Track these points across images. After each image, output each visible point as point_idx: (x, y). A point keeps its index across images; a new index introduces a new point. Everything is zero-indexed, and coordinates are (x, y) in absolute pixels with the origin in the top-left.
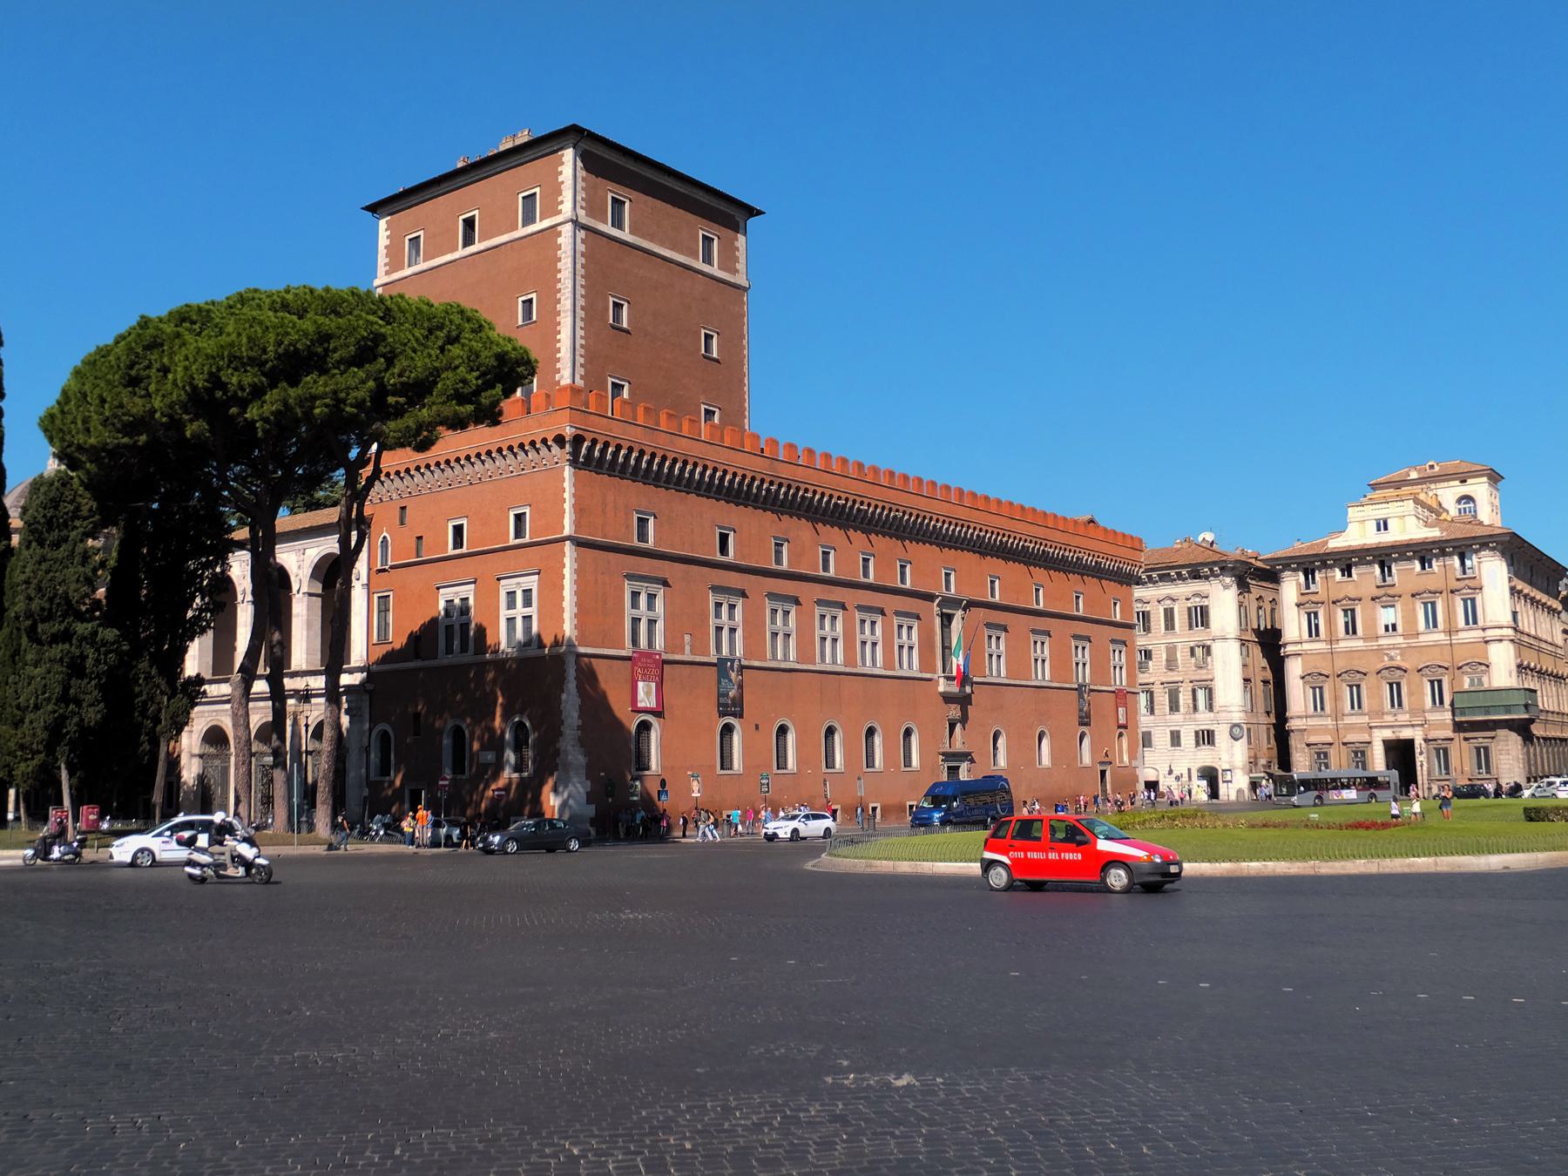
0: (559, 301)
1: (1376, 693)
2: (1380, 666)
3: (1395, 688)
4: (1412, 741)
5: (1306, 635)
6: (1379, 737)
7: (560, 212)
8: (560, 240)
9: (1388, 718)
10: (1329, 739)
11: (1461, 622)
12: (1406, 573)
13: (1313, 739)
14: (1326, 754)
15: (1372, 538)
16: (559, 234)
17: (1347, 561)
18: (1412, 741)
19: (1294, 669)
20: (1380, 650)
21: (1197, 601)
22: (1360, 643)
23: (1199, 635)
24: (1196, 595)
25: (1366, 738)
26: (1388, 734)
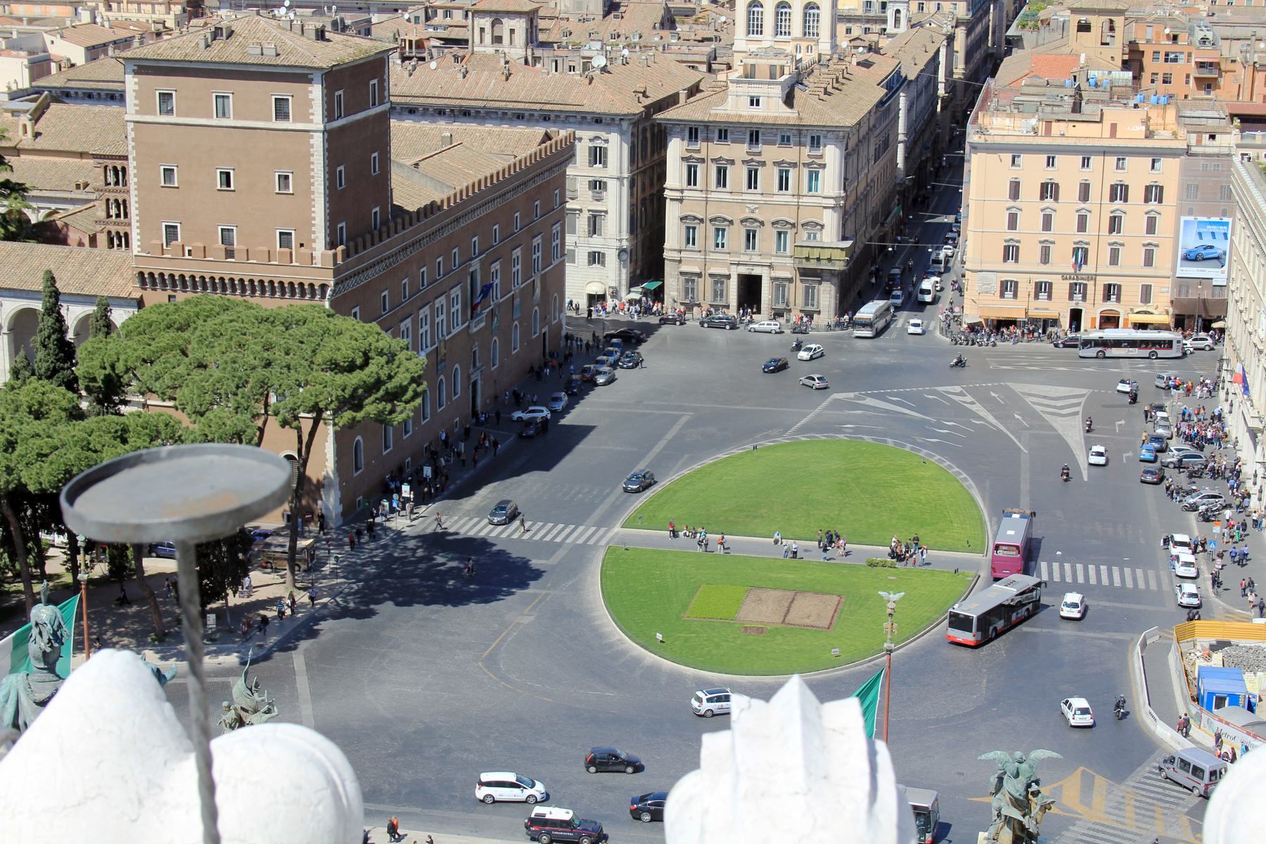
0: (313, 184)
1: (735, 236)
2: (743, 216)
3: (750, 237)
4: (760, 278)
5: (685, 185)
6: (735, 272)
7: (311, 121)
8: (312, 141)
9: (744, 259)
10: (698, 271)
11: (805, 190)
12: (771, 152)
13: (684, 268)
14: (693, 281)
15: (746, 113)
16: (312, 137)
17: (724, 132)
18: (758, 279)
19: (673, 213)
20: (743, 202)
21: (598, 143)
22: (728, 196)
23: (597, 172)
24: (597, 138)
25: (724, 271)
26: (744, 270)
